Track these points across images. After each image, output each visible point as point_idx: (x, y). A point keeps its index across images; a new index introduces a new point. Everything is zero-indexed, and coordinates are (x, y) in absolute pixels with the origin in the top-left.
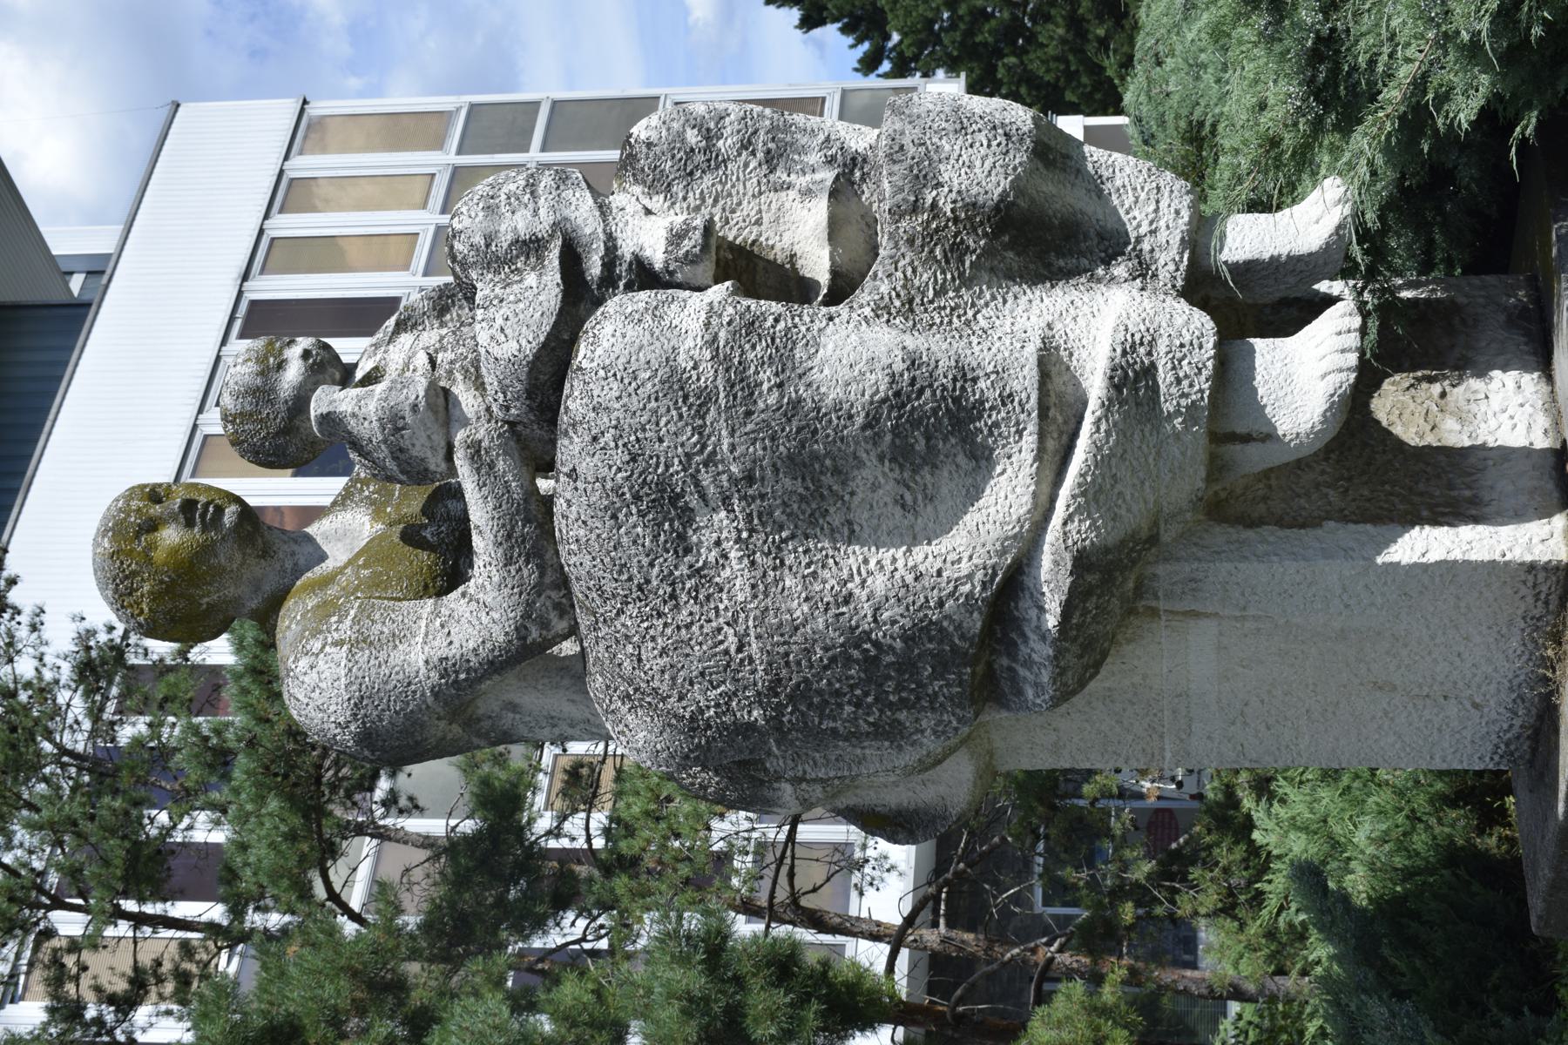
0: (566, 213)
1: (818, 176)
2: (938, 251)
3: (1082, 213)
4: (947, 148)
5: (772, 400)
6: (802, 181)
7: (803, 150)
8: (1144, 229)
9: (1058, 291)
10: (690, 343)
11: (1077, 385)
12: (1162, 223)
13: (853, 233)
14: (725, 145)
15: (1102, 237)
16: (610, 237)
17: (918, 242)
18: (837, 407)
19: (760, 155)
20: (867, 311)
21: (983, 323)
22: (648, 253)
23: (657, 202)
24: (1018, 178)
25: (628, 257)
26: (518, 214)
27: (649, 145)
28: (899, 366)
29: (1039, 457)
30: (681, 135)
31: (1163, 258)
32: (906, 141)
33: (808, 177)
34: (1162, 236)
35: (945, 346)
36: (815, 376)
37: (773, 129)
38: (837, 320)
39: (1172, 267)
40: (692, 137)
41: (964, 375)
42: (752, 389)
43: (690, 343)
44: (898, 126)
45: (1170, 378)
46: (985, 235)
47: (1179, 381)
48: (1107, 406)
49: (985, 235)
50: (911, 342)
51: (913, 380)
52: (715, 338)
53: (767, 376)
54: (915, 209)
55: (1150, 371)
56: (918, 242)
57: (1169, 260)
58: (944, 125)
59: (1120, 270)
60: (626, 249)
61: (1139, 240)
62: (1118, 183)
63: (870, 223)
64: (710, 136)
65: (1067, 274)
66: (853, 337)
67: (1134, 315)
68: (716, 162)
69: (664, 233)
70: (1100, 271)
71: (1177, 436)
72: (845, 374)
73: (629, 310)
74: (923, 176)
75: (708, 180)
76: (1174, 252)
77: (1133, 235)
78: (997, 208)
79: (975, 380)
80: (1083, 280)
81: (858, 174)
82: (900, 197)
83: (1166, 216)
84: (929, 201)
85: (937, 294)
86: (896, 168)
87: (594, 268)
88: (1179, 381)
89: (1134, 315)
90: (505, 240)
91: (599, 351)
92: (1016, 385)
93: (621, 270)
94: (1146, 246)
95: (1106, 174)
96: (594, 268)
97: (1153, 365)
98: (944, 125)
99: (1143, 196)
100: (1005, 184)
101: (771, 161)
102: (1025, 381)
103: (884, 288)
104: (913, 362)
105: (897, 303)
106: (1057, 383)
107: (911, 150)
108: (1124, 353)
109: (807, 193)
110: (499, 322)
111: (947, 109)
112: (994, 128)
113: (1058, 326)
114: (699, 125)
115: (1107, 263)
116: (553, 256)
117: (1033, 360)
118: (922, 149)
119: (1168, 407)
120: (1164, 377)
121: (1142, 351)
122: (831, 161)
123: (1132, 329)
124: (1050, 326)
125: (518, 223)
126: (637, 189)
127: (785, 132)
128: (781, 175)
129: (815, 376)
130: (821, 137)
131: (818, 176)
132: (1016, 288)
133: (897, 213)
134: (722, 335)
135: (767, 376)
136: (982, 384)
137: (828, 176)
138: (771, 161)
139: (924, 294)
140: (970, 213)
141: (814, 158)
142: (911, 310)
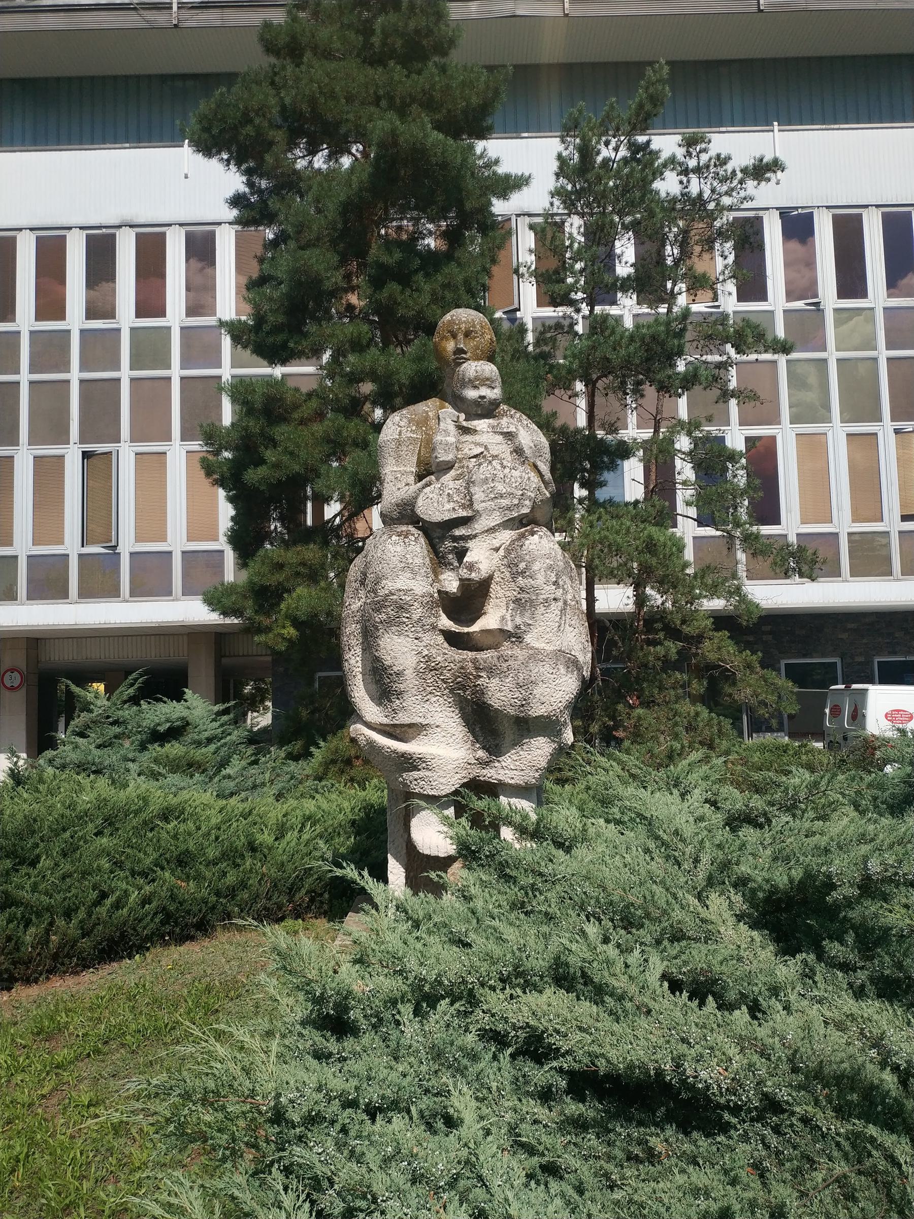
0: (484, 515)
1: (509, 623)
2: (460, 679)
3: (504, 738)
4: (507, 681)
5: (377, 619)
6: (508, 618)
7: (522, 615)
8: (504, 764)
9: (461, 728)
10: (390, 584)
11: (413, 738)
12: (507, 772)
13: (489, 640)
14: (521, 581)
15: (496, 746)
16: (475, 536)
17: (462, 671)
18: (378, 645)
19: (519, 596)
20: (426, 652)
21: (435, 699)
22: (468, 554)
23: (502, 552)
24: (501, 711)
25: (467, 545)
26: (482, 494)
27: (522, 546)
28: (395, 669)
29: (381, 724)
30: (523, 560)
31: (493, 771)
32: (510, 663)
33: (509, 618)
34: (502, 772)
35: (411, 686)
36: (386, 636)
37: (531, 601)
38: (416, 641)
39: (489, 775)
40: (522, 565)
41: (399, 694)
42: (378, 611)
43: (390, 584)
44: (520, 657)
45: (416, 777)
46: (472, 699)
47: (416, 780)
48: (394, 751)
49: (472, 699)
50: (409, 673)
51: (391, 675)
52: (393, 594)
53: (383, 616)
54: (477, 669)
55: (416, 768)
56: (462, 671)
57: (492, 774)
58: (521, 678)
59: (481, 753)
60: (471, 544)
61: (498, 761)
62: (521, 753)
63: (496, 647)
64: (523, 572)
65: (472, 731)
66: (406, 649)
67: (441, 762)
68: (514, 576)
69: (476, 559)
70: (478, 745)
71: (397, 779)
72: (389, 647)
73: (408, 556)
74: (491, 671)
75: (508, 574)
76: (495, 776)
77: (500, 759)
78: (485, 703)
79: (398, 699)
80: (471, 738)
81: (514, 639)
82: (482, 662)
83: (511, 774)
84: (482, 674)
85: (443, 680)
86: (495, 659)
87: (458, 532)
88: (416, 780)
89: (441, 762)
90: (472, 490)
91: (390, 546)
92: (400, 715)
93: (462, 544)
94: (497, 764)
95: (524, 747)
96: (458, 532)
97: (419, 770)
98: (521, 678)
99: (518, 763)
100: (496, 706)
101: (517, 601)
102: (403, 718)
103: (439, 659)
104: (399, 674)
105: (433, 664)
106: (410, 731)
107: (505, 665)
108: (420, 759)
109: (503, 618)
110: (431, 496)
111: (533, 679)
112: (525, 700)
113: (439, 730)
114: (527, 568)
115: (483, 748)
116: (463, 513)
117: (413, 721)
118: (506, 669)
119: (404, 775)
120: (415, 774)
121: (424, 765)
122: (517, 627)
123: (433, 761)
124: (437, 727)
125: (478, 494)
126: (508, 543)
127: (531, 606)
128: (512, 606)
129: (386, 636)
130: (530, 622)
131: (509, 623)
132: (457, 712)
133: (474, 661)
134: (395, 597)
135: (383, 616)
136: (397, 701)
137: (509, 627)
138: (517, 601)
139: (441, 674)
140: (480, 692)
141: (518, 620)
142: (431, 670)
